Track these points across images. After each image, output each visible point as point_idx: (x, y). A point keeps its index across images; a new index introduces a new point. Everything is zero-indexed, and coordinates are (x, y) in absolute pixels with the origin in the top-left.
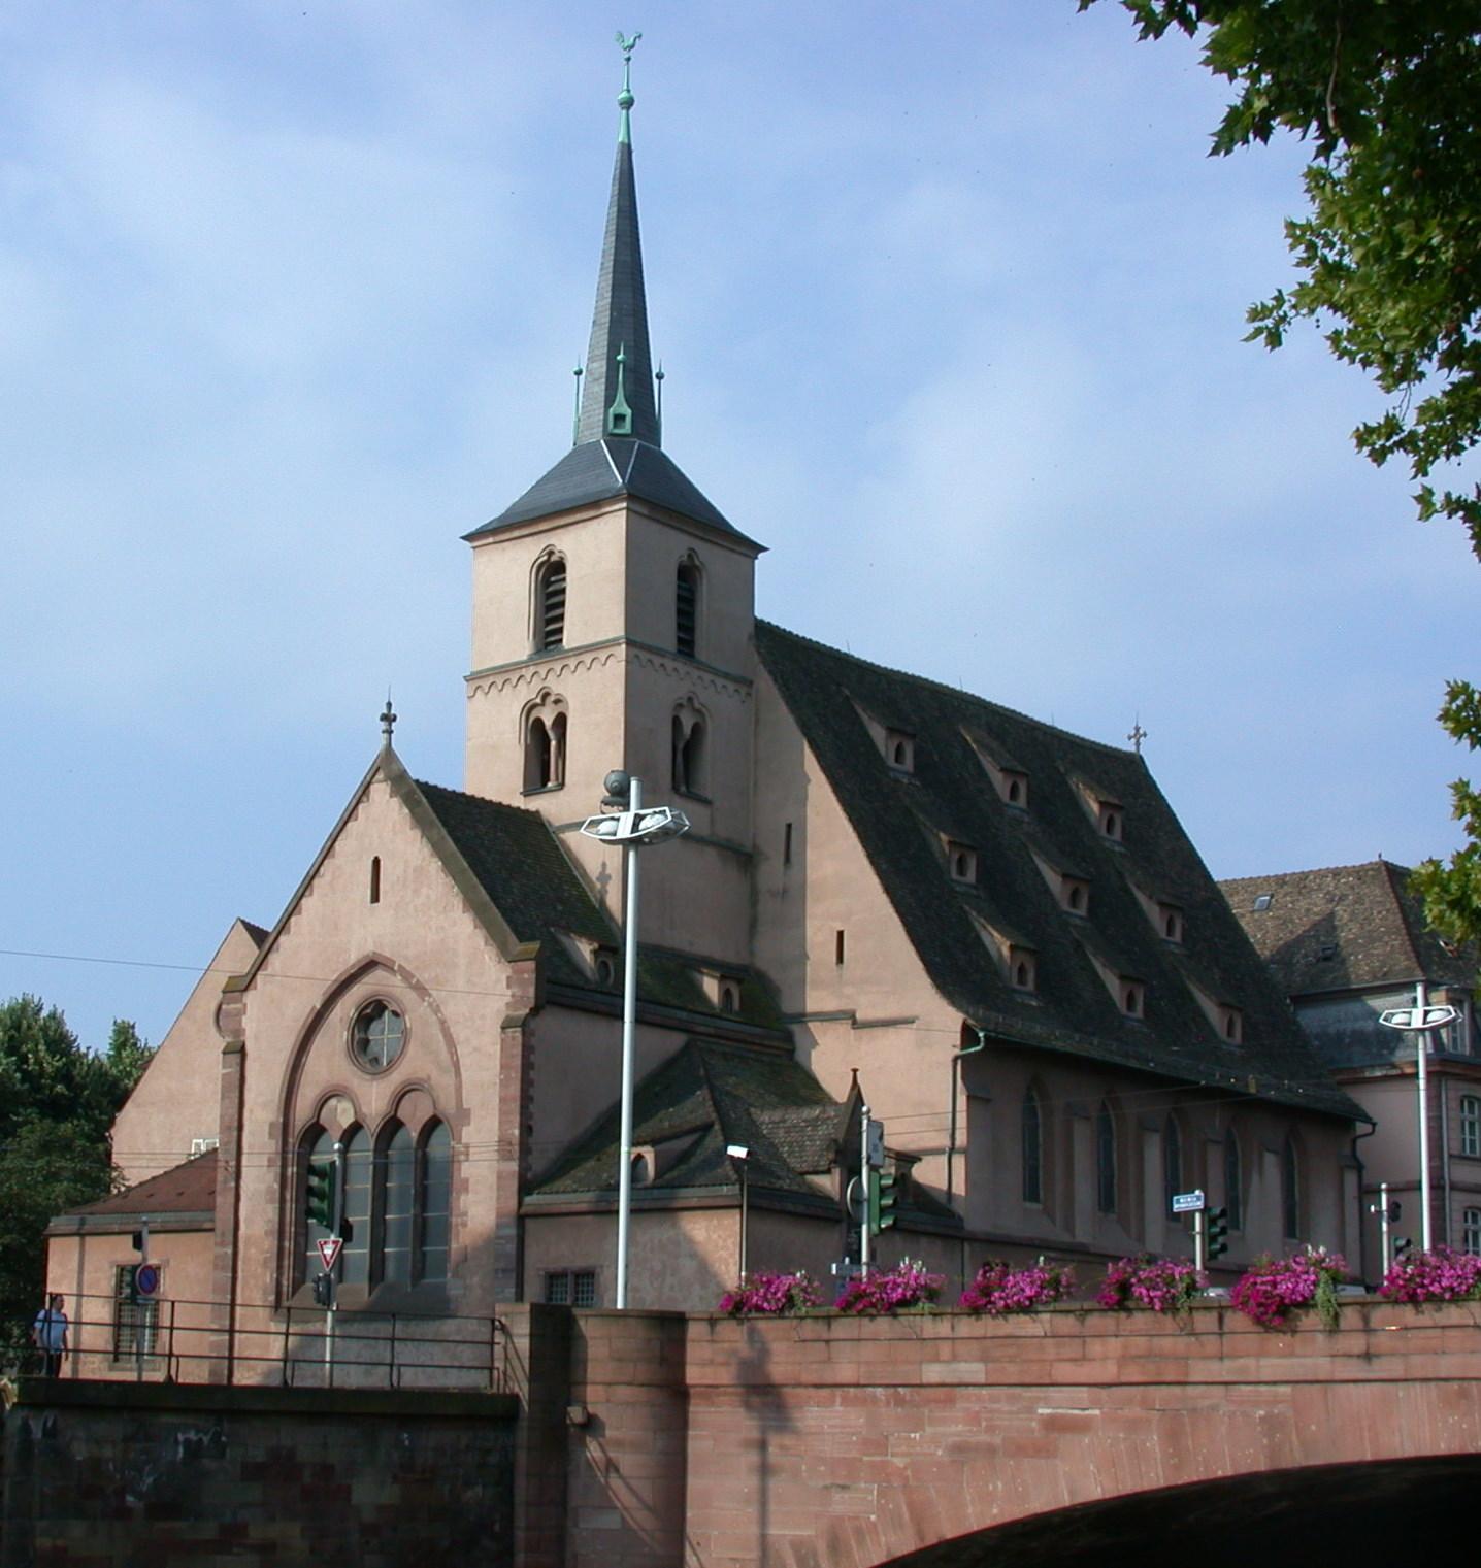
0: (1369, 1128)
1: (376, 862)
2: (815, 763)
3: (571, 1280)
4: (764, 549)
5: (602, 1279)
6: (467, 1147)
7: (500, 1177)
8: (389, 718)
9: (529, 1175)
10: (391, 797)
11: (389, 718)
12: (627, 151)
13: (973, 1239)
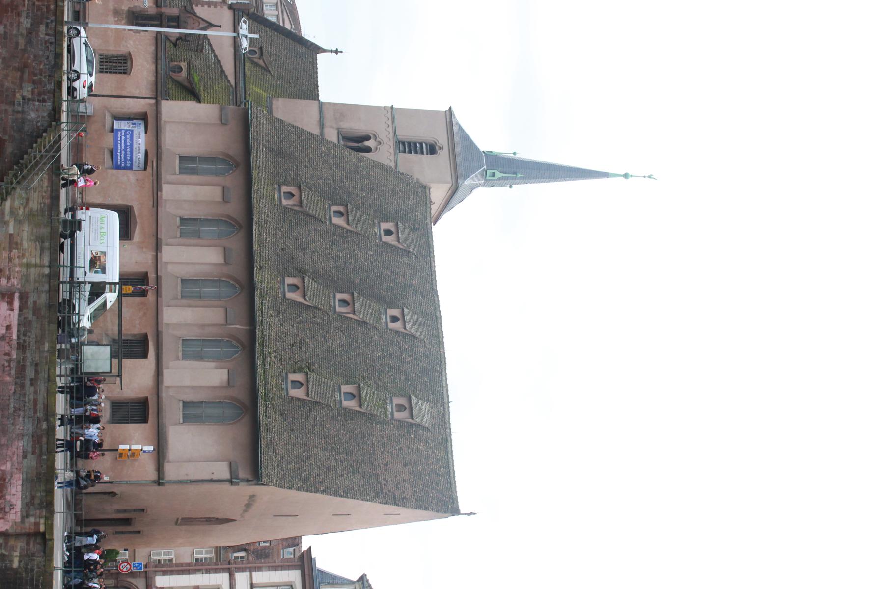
2: (365, 153)
8: (337, 52)
11: (337, 52)
12: (605, 175)
13: (157, 105)
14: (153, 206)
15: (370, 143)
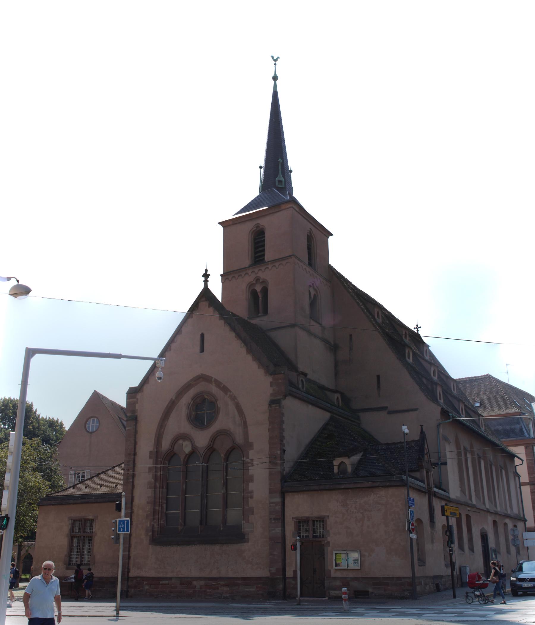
0: (520, 462)
3: (311, 523)
4: (332, 235)
6: (252, 460)
7: (271, 474)
9: (284, 473)
10: (209, 307)
14: (479, 512)
15: (313, 293)
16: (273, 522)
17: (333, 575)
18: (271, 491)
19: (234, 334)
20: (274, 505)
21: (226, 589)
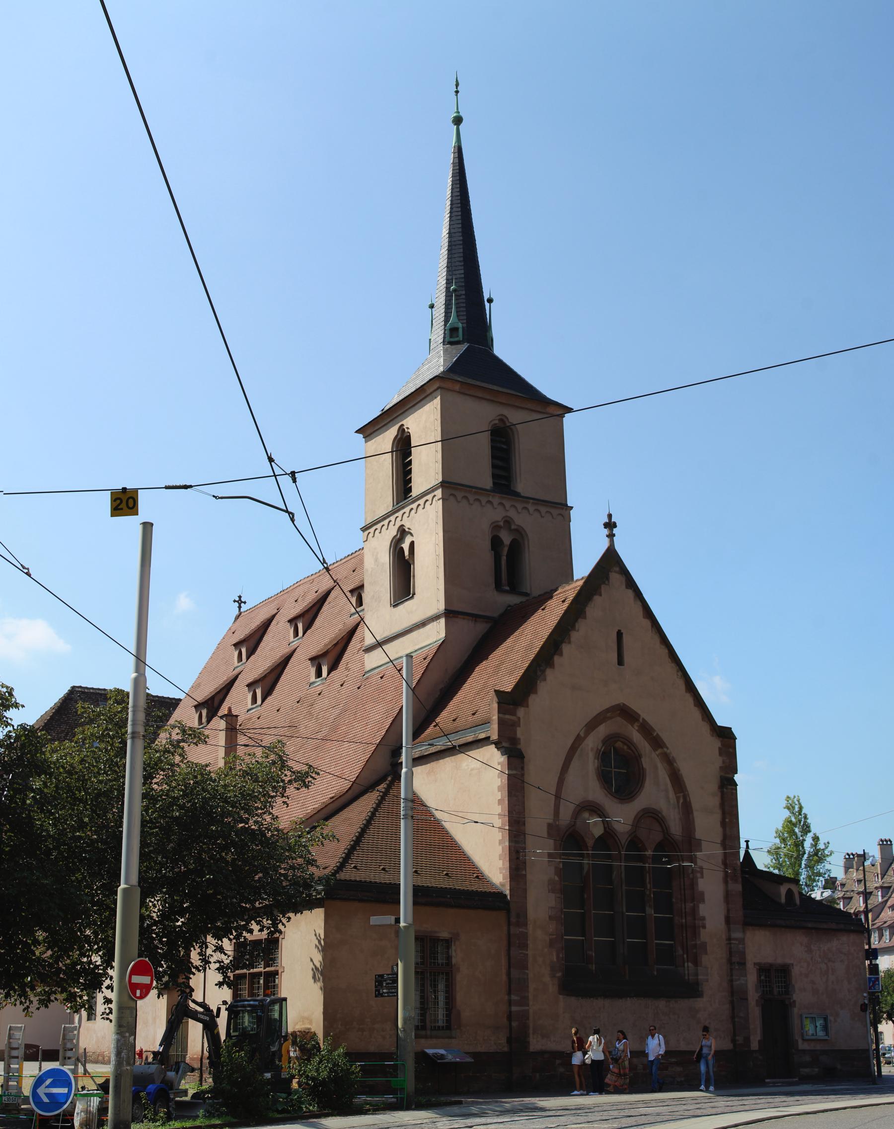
1: (620, 635)
5: (793, 974)
8: (610, 525)
11: (610, 525)
16: (737, 967)
17: (802, 1046)
18: (728, 920)
19: (667, 651)
20: (737, 942)
21: (679, 1069)
